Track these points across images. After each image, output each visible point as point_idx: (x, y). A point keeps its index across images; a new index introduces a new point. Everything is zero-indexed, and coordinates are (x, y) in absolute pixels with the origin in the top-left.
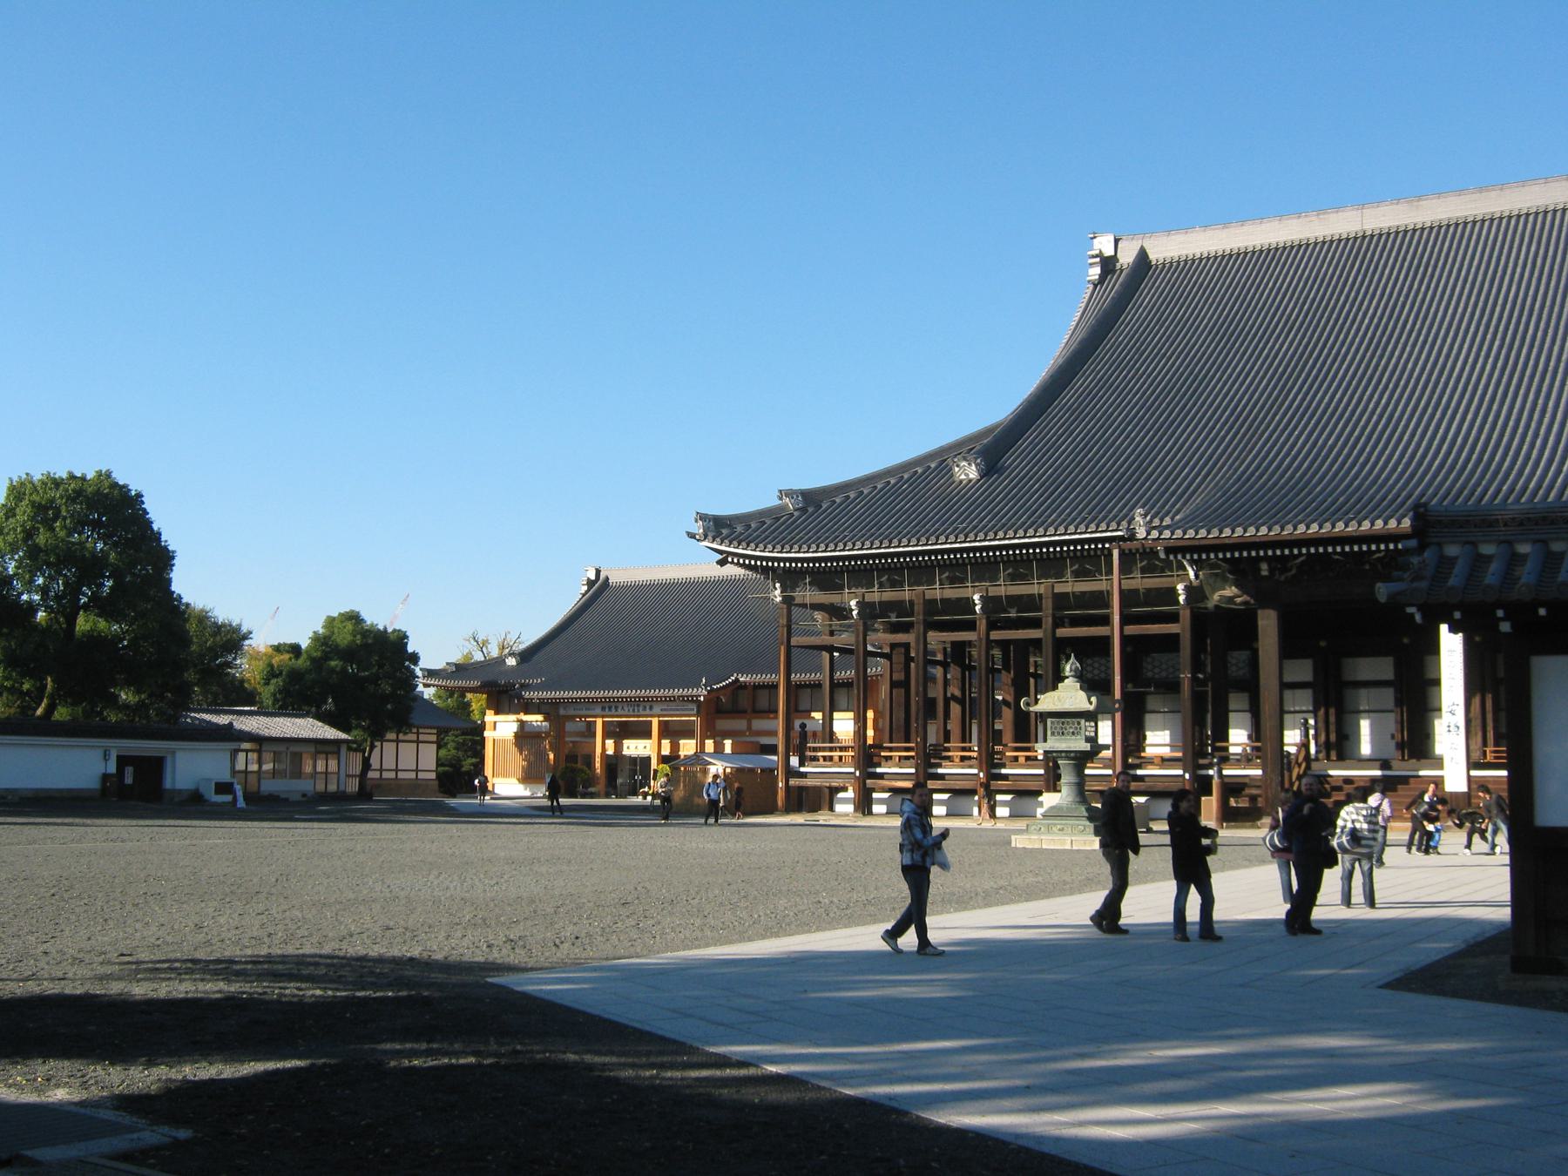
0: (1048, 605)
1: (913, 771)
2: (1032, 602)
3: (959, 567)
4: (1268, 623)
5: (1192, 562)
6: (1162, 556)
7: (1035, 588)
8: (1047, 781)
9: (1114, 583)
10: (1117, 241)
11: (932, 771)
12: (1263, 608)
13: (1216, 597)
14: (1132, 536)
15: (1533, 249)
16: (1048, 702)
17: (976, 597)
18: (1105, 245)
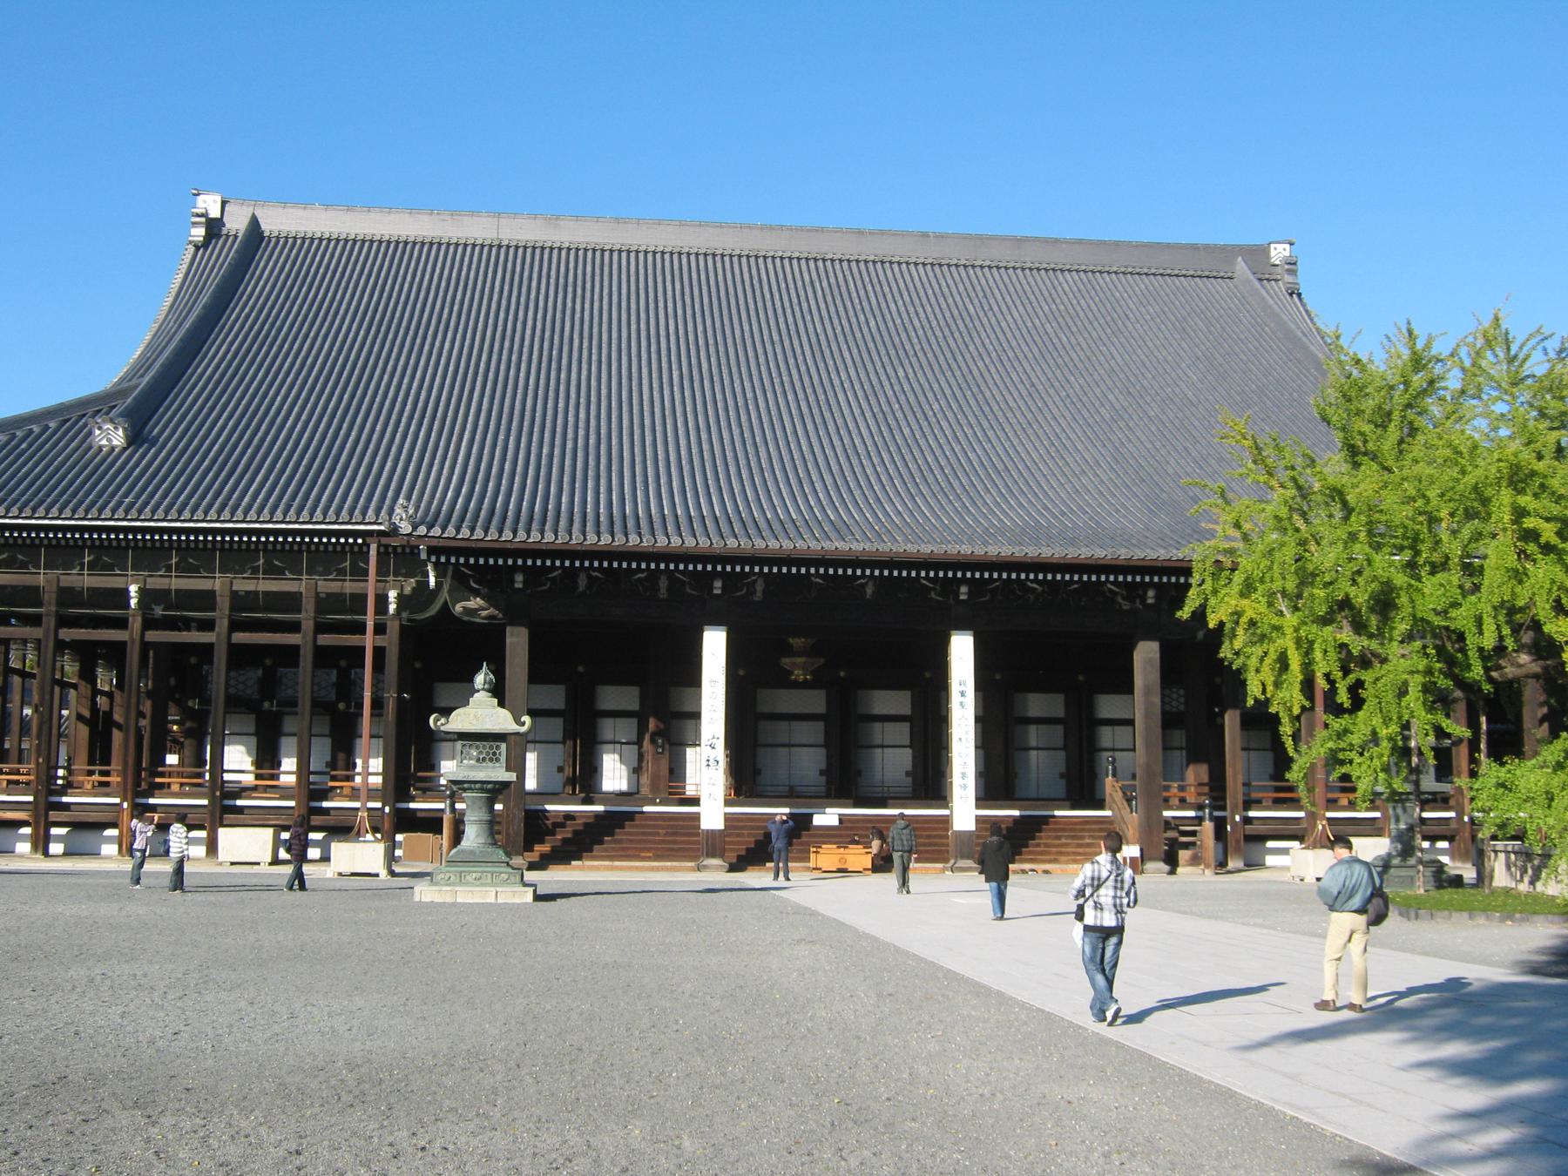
0: (224, 604)
1: (31, 798)
2: (206, 599)
3: (114, 550)
4: (517, 641)
5: (437, 565)
6: (424, 556)
7: (217, 583)
8: (212, 814)
9: (371, 587)
10: (224, 203)
11: (55, 799)
12: (512, 624)
13: (458, 608)
14: (394, 531)
15: (678, 287)
16: (460, 721)
17: (133, 589)
18: (210, 204)
